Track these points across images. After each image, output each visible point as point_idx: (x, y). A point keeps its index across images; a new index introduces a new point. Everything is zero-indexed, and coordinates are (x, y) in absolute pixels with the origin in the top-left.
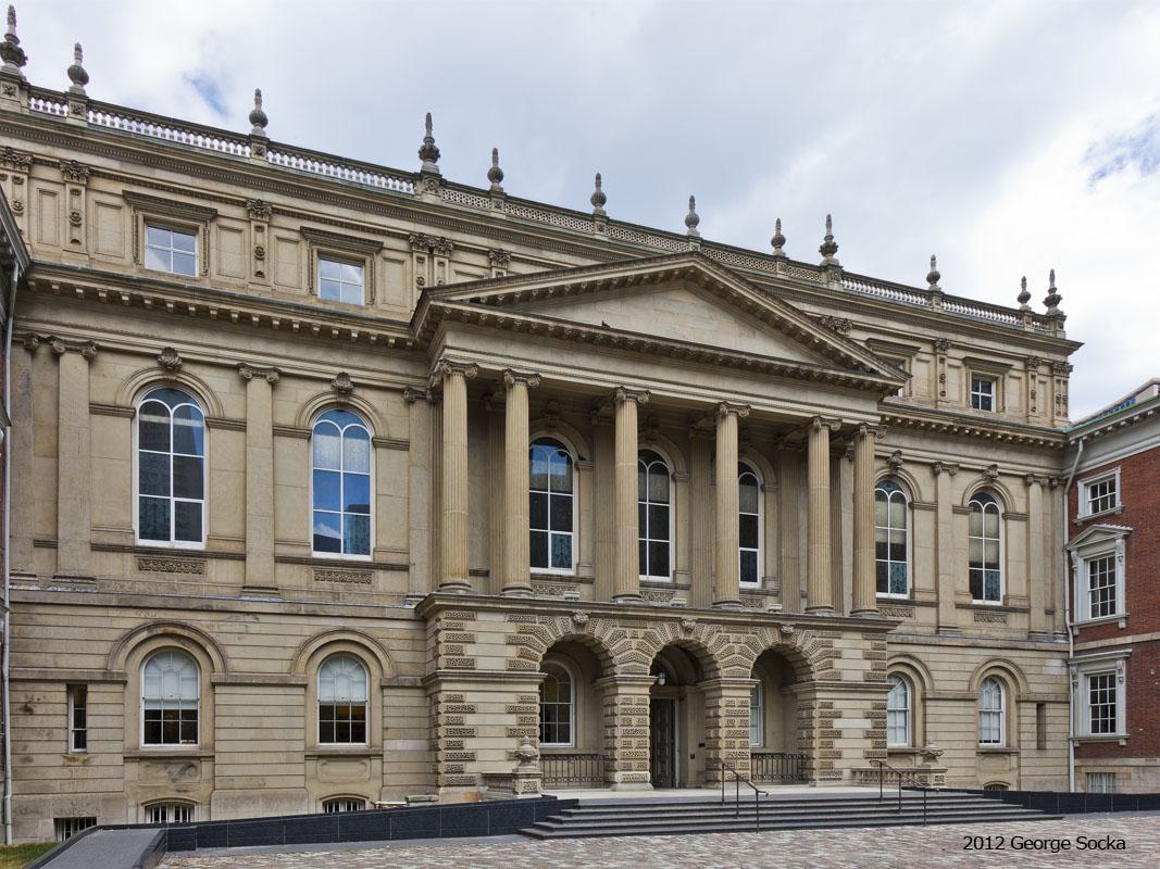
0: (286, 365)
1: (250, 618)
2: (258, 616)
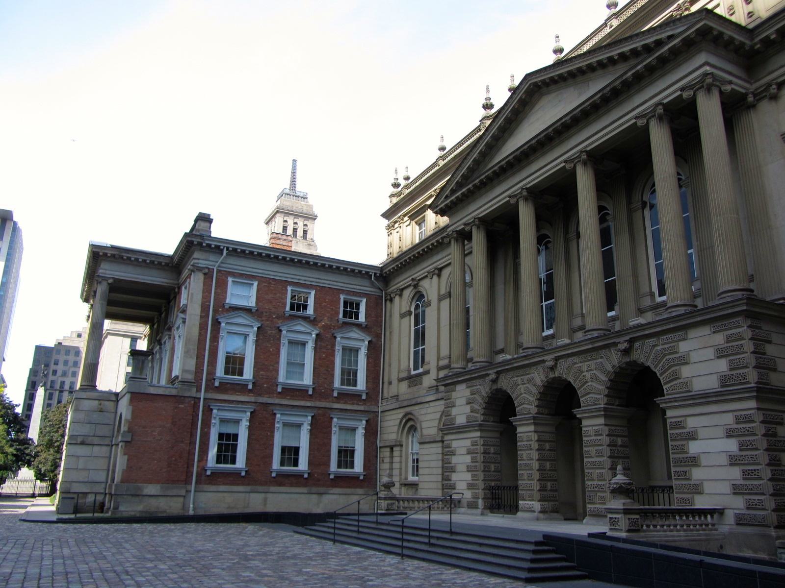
0: (439, 264)
1: (427, 405)
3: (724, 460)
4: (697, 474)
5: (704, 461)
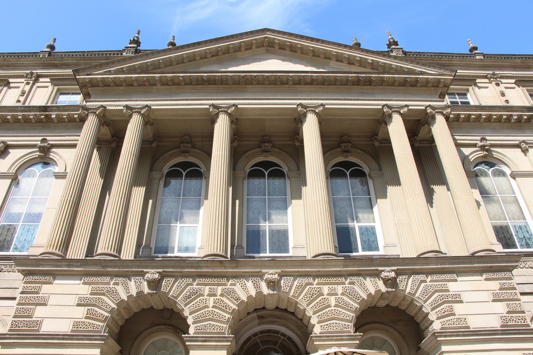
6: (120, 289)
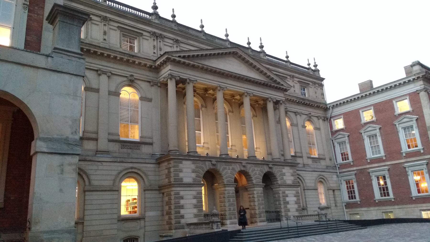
1: (99, 164)
2: (102, 163)
3: (294, 203)
4: (288, 206)
5: (290, 203)
6: (203, 166)
